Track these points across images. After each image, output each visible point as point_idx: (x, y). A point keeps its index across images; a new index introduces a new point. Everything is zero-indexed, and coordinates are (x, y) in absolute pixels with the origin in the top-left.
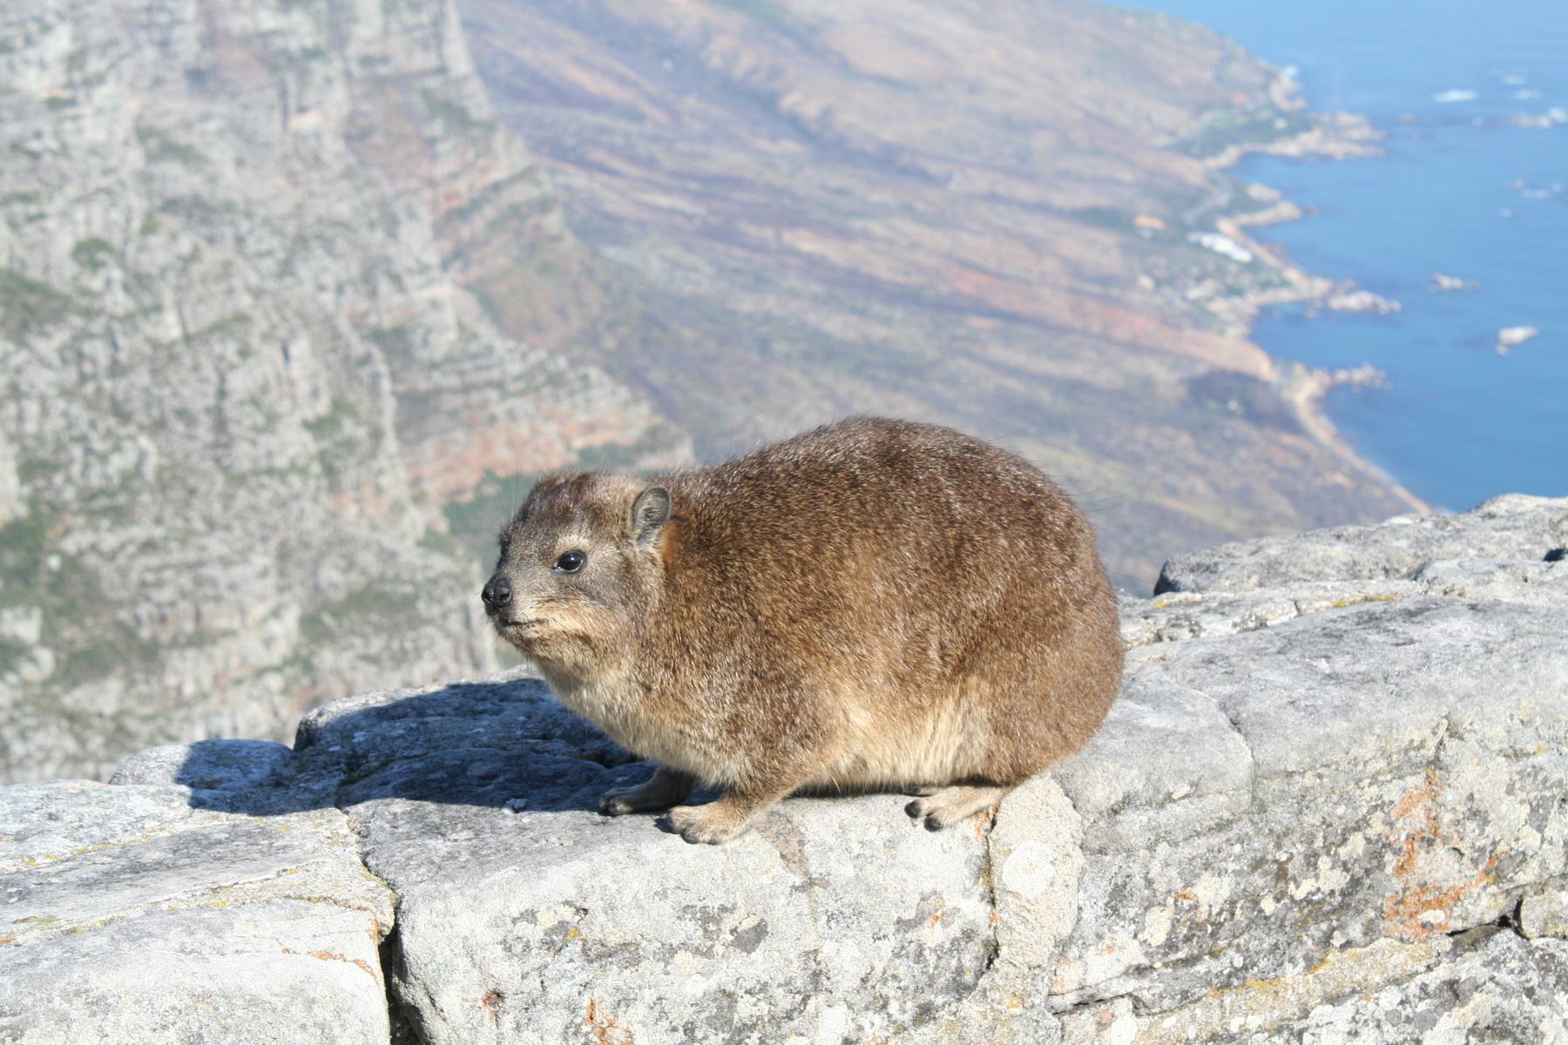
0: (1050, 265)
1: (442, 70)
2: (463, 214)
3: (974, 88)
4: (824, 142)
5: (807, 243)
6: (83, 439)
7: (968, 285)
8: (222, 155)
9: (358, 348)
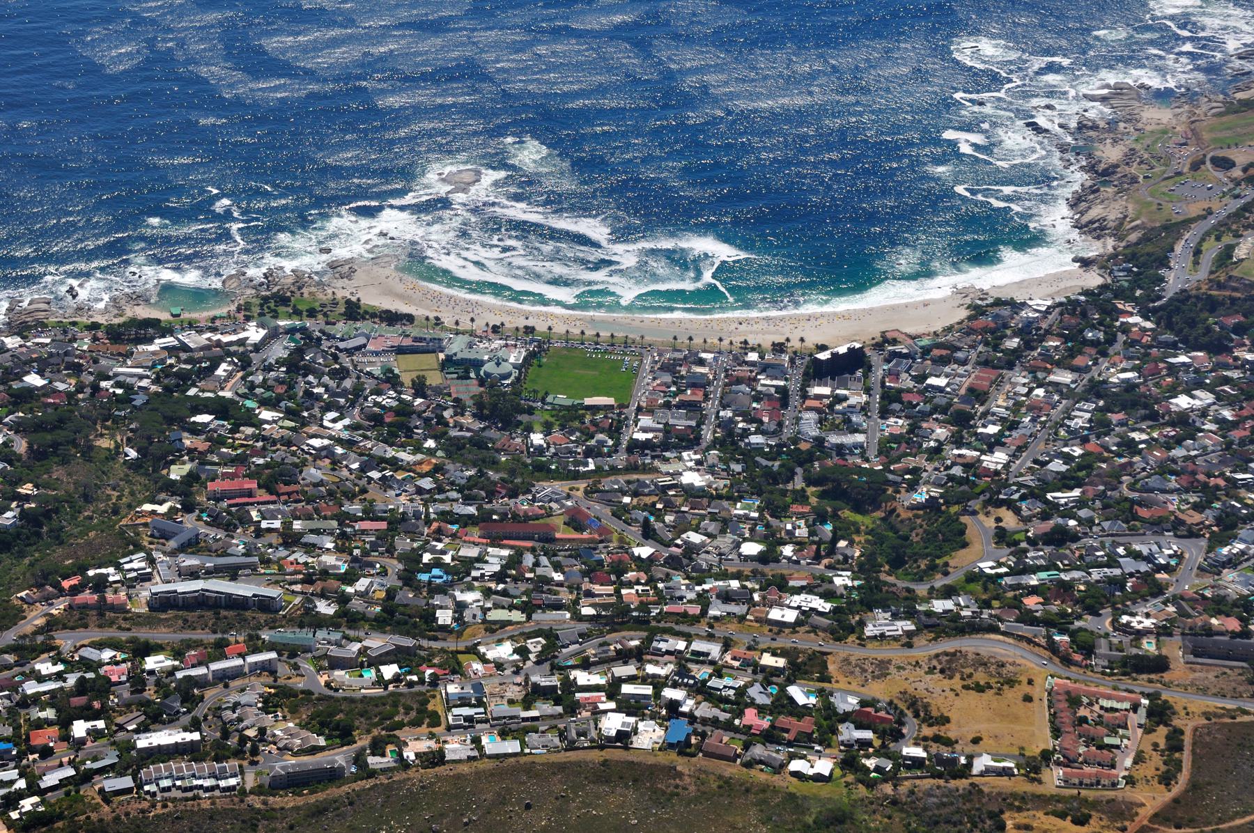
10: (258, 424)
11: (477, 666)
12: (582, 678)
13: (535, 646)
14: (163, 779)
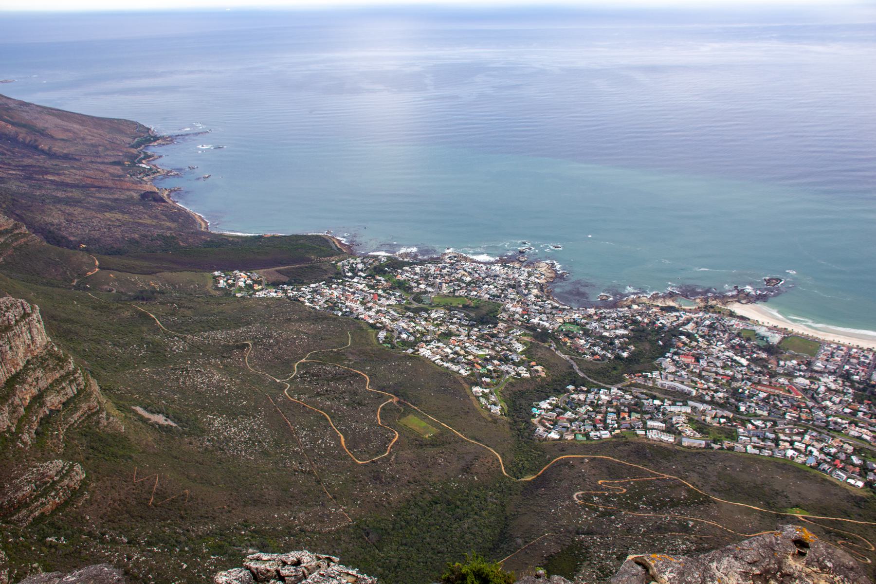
0: (107, 175)
3: (83, 139)
4: (51, 155)
5: (51, 178)
7: (89, 181)
10: (698, 341)
11: (750, 426)
12: (782, 437)
13: (769, 424)
14: (653, 435)
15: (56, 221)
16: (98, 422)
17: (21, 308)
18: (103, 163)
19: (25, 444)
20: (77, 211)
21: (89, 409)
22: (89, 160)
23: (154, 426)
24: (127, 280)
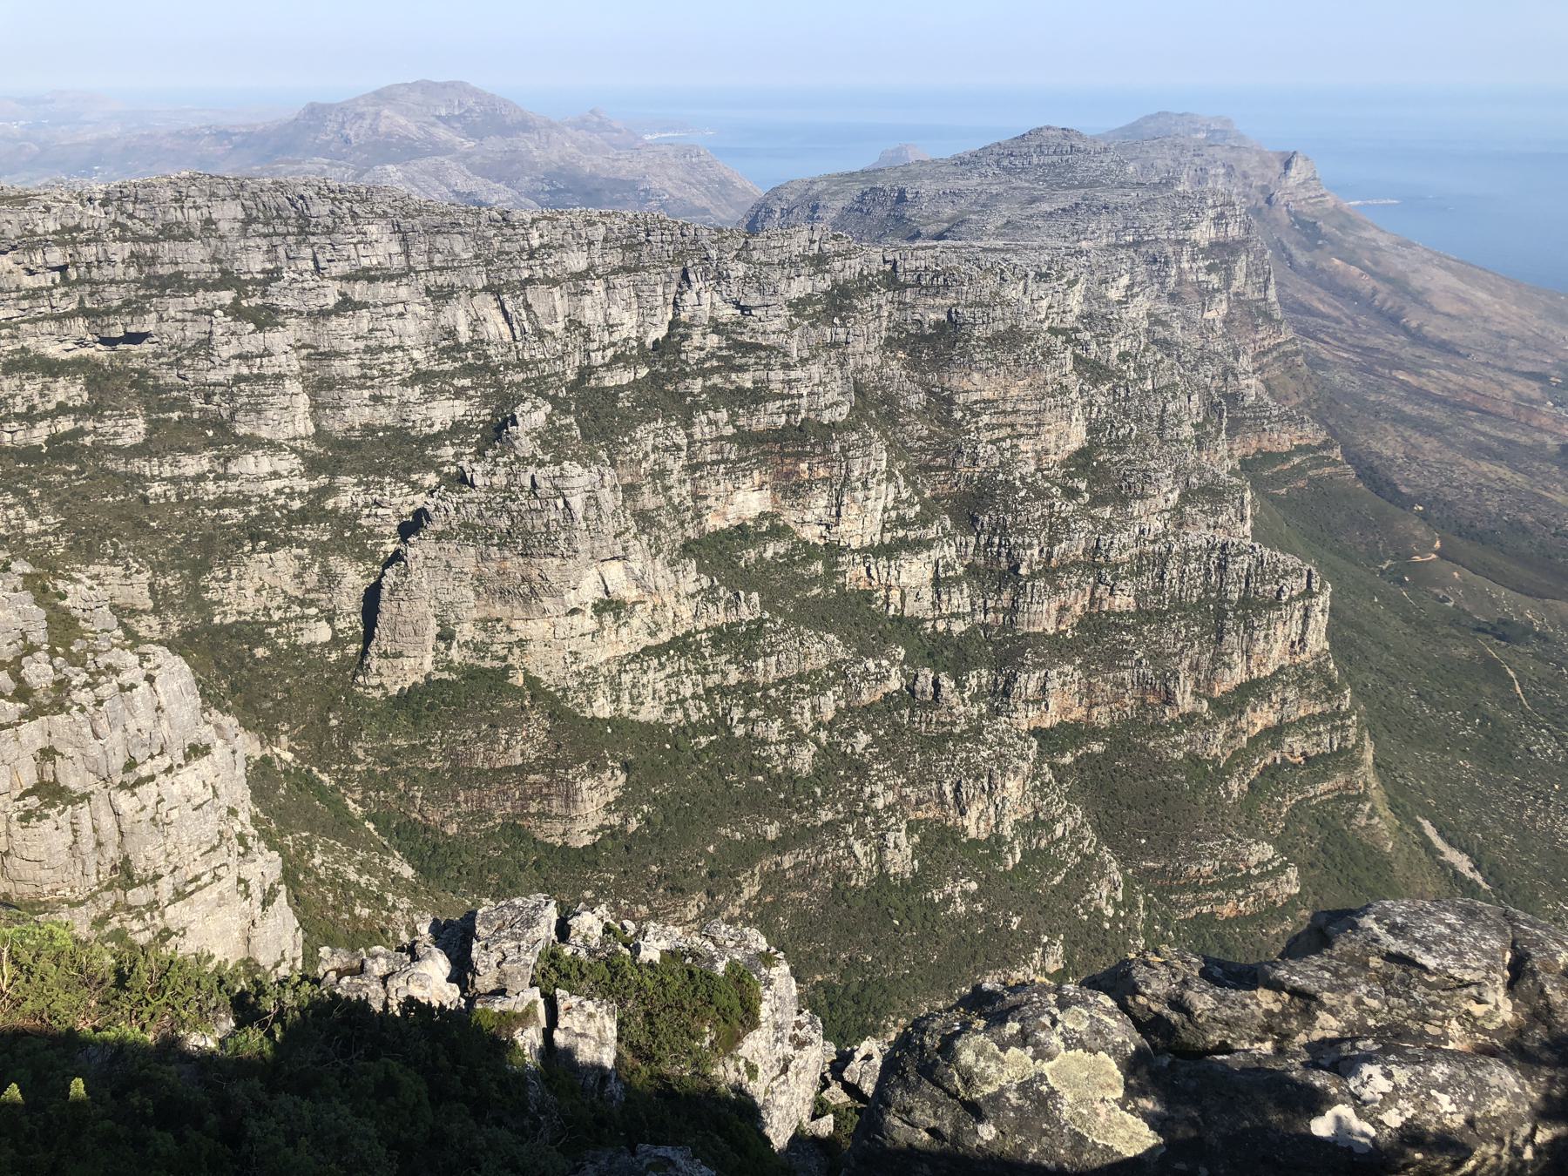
1: (1265, 299)
2: (1264, 354)
3: (1486, 320)
4: (1417, 338)
5: (1402, 376)
6: (1111, 422)
8: (1177, 325)
9: (1217, 400)
15: (1389, 453)
16: (1351, 816)
17: (1305, 580)
18: (1509, 370)
19: (1229, 794)
20: (1430, 445)
21: (1346, 787)
22: (1483, 360)
23: (1445, 866)
24: (1483, 592)
